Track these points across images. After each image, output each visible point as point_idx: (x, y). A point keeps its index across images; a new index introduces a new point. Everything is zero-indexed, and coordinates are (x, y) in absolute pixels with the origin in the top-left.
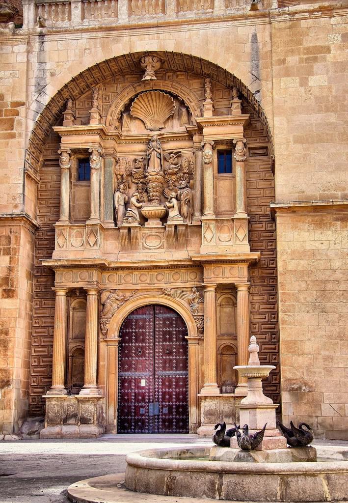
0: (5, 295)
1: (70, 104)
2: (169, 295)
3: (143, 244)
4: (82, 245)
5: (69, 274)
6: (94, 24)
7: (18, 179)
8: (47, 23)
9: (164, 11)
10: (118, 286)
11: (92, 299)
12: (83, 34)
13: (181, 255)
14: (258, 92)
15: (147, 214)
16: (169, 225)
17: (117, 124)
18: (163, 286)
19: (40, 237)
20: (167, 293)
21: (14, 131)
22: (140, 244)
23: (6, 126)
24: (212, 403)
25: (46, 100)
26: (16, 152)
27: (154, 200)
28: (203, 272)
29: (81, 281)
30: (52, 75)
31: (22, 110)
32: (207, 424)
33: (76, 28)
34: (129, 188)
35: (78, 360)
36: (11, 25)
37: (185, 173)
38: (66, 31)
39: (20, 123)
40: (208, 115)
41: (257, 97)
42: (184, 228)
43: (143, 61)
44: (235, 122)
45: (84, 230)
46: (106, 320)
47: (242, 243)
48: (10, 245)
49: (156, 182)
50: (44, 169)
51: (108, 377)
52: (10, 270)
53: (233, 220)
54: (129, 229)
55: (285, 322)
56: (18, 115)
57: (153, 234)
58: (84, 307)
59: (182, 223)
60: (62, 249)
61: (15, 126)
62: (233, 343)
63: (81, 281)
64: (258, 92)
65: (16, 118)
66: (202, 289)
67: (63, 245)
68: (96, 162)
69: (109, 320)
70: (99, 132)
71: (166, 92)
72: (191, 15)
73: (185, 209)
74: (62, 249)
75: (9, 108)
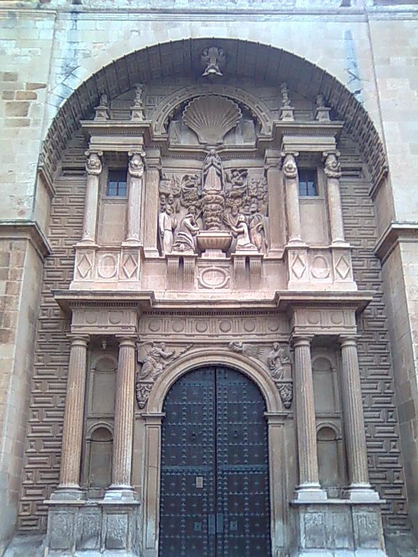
1: (104, 99)
2: (240, 352)
3: (199, 283)
4: (115, 276)
10: (164, 337)
11: (127, 354)
12: (130, 14)
13: (264, 293)
14: (358, 92)
15: (206, 242)
16: (238, 256)
18: (232, 340)
19: (50, 266)
20: (238, 349)
21: (28, 117)
22: (196, 281)
23: (17, 111)
24: (316, 515)
25: (75, 84)
26: (29, 148)
27: (212, 226)
29: (112, 325)
32: (311, 550)
33: (120, 7)
34: (178, 212)
35: (101, 447)
37: (252, 197)
39: (36, 108)
41: (358, 97)
42: (260, 261)
43: (205, 53)
44: (324, 131)
45: (119, 255)
46: (145, 385)
47: (345, 281)
48: (8, 266)
49: (218, 203)
50: (62, 178)
51: (147, 473)
52: (5, 302)
53: (331, 250)
54: (181, 259)
57: (214, 268)
58: (113, 368)
59: (256, 253)
60: (83, 280)
61: (29, 111)
62: (331, 422)
63: (112, 325)
64: (358, 92)
65: (32, 102)
66: (293, 343)
67: (87, 275)
69: (150, 385)
70: (143, 132)
73: (258, 237)
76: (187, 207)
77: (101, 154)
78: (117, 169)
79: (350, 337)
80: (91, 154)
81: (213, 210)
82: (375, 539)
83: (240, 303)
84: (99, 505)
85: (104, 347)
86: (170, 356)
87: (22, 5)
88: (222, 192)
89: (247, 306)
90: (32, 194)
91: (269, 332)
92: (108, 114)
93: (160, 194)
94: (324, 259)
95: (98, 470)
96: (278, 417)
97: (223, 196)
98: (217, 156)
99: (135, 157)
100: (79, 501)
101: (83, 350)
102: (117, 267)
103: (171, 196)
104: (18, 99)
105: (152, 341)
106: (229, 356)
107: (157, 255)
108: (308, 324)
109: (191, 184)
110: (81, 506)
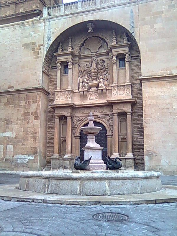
0: (35, 119)
1: (61, 44)
2: (100, 118)
4: (65, 99)
5: (59, 110)
6: (70, 12)
7: (40, 74)
8: (51, 14)
9: (95, 5)
14: (133, 32)
17: (79, 51)
18: (98, 114)
20: (99, 117)
21: (39, 55)
22: (88, 98)
23: (36, 54)
25: (50, 43)
26: (40, 64)
27: (94, 80)
28: (112, 108)
30: (53, 33)
31: (42, 47)
36: (39, 17)
37: (106, 69)
38: (58, 16)
39: (41, 52)
40: (114, 43)
41: (133, 34)
42: (105, 90)
44: (125, 46)
53: (125, 85)
54: (84, 91)
55: (146, 127)
56: (40, 49)
57: (93, 93)
59: (104, 88)
60: (57, 101)
62: (125, 136)
64: (133, 32)
65: (40, 50)
68: (70, 66)
71: (98, 37)
72: (106, 5)
73: (106, 82)
74: (57, 101)
75: (37, 47)
76: (87, 74)
77: (60, 62)
78: (65, 65)
79: (128, 112)
80: (57, 63)
81: (94, 75)
82: (132, 167)
83: (99, 104)
84: (63, 159)
85: (64, 118)
86: (81, 120)
87: (35, 20)
88: (97, 69)
89: (100, 104)
90: (41, 78)
91: (108, 111)
92: (62, 49)
93: (79, 71)
94: (123, 89)
95: (62, 151)
96: (110, 135)
97: (97, 70)
98: (96, 57)
99: (69, 62)
100: (58, 158)
101: (58, 120)
102: (66, 96)
103: (82, 71)
104: (36, 50)
105: (76, 116)
106: (97, 119)
107: (77, 91)
108: (117, 109)
109: (88, 67)
110: (58, 159)
